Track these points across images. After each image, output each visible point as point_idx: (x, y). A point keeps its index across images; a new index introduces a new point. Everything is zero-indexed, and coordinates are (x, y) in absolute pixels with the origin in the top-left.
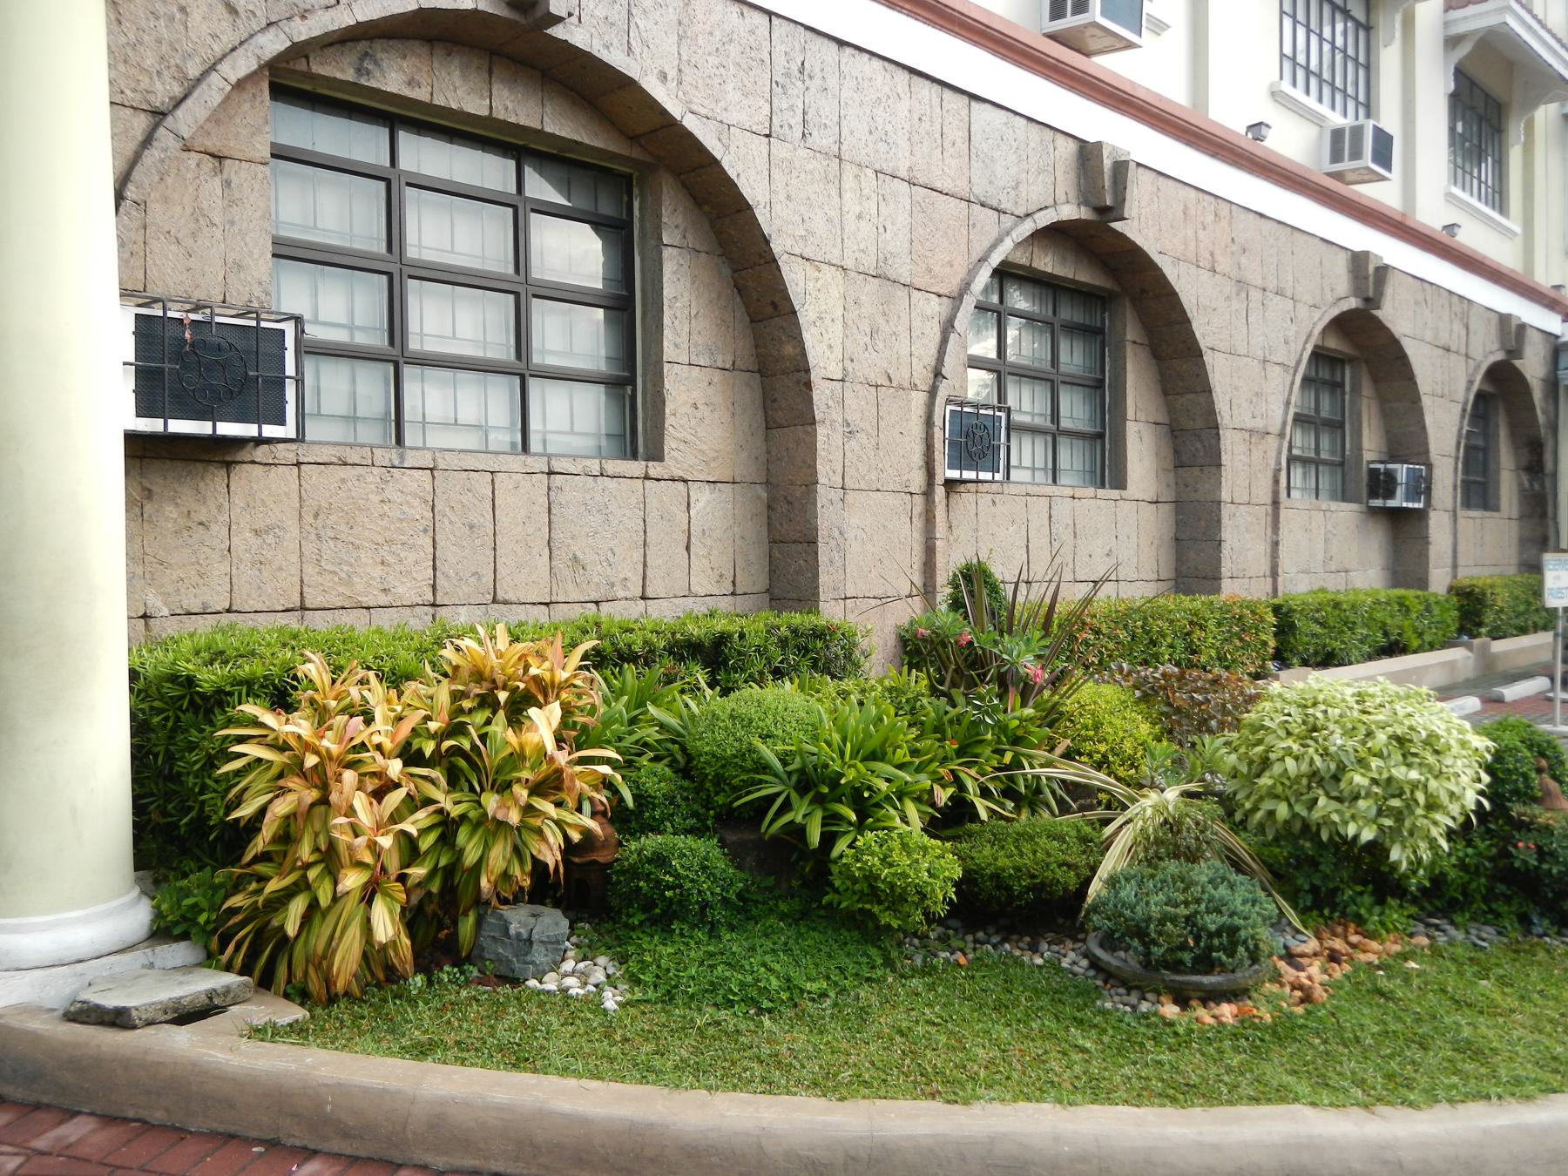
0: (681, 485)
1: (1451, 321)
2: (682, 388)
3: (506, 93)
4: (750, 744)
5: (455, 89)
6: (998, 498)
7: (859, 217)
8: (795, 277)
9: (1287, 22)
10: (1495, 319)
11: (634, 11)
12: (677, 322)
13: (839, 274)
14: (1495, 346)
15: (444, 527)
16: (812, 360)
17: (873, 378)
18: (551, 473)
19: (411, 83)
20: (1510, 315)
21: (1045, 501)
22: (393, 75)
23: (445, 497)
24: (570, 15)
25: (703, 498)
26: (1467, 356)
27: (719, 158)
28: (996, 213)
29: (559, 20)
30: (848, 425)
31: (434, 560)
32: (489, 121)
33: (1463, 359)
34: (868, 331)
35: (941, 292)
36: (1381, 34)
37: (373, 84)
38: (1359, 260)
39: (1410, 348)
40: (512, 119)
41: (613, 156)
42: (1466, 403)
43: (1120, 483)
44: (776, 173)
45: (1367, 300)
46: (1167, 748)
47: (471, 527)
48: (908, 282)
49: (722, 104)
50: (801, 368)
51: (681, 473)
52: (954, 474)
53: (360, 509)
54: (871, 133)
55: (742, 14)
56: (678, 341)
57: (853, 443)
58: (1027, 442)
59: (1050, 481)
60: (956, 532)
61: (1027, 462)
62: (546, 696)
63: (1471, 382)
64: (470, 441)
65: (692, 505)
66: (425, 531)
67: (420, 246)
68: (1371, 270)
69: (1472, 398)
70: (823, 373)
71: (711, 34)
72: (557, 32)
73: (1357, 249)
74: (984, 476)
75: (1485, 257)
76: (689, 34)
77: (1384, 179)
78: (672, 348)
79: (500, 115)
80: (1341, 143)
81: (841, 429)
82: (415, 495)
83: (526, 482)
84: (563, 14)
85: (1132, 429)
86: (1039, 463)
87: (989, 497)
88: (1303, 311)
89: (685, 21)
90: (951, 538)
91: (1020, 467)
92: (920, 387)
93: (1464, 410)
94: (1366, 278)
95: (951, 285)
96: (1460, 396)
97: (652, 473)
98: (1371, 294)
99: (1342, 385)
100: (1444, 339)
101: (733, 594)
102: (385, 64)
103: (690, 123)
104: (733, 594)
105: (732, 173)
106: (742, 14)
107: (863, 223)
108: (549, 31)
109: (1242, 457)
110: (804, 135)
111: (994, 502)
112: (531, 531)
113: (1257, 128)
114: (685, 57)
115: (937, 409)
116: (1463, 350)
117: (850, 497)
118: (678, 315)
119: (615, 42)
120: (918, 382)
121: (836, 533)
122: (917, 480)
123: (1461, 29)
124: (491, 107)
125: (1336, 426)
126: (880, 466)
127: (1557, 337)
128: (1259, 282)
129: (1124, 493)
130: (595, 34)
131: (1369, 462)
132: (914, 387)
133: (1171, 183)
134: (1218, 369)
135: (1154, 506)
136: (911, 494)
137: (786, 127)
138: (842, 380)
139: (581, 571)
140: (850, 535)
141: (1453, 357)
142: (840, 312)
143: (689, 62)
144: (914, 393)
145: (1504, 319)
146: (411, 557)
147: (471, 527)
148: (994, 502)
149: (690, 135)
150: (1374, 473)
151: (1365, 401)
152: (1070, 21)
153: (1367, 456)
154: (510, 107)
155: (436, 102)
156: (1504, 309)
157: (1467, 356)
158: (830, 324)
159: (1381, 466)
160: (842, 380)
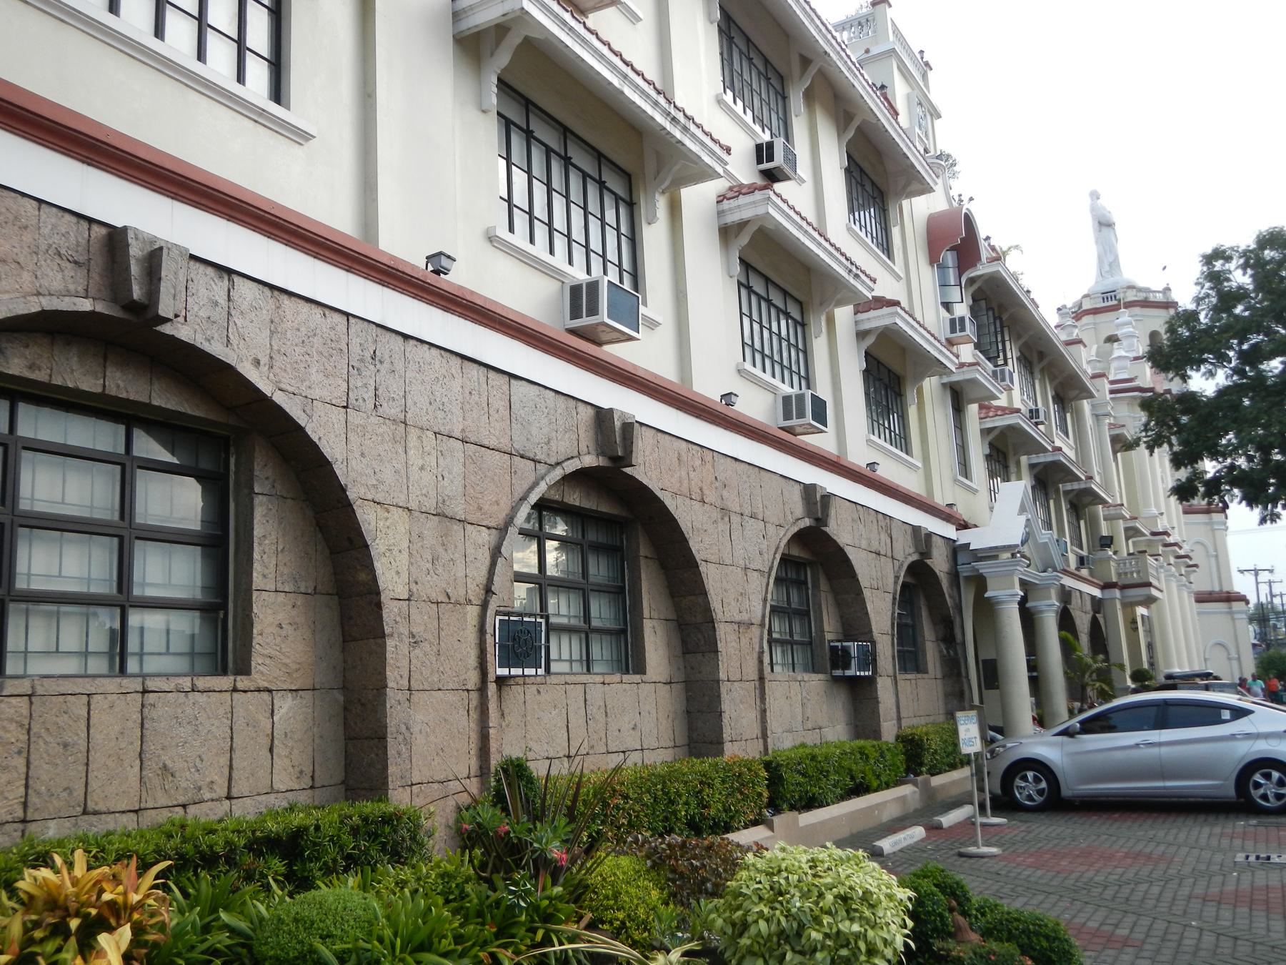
0: (266, 696)
1: (879, 533)
2: (269, 611)
3: (118, 374)
4: (311, 945)
5: (72, 371)
6: (542, 688)
7: (422, 468)
8: (367, 517)
9: (746, 321)
10: (909, 530)
11: (233, 312)
12: (265, 556)
13: (405, 514)
14: (912, 550)
15: (39, 748)
16: (382, 582)
17: (434, 597)
18: (145, 692)
19: (32, 367)
21: (581, 688)
22: (16, 361)
23: (41, 720)
24: (176, 316)
25: (285, 706)
26: (892, 558)
27: (303, 425)
28: (532, 463)
29: (167, 320)
30: (414, 636)
31: (27, 779)
32: (103, 396)
34: (430, 558)
36: (813, 328)
39: (852, 554)
40: (123, 395)
41: (212, 423)
42: (895, 594)
43: (640, 669)
44: (352, 436)
45: (817, 520)
46: (673, 910)
47: (66, 745)
48: (463, 517)
49: (307, 383)
50: (372, 592)
51: (266, 684)
52: (503, 672)
54: (431, 403)
55: (324, 315)
56: (266, 572)
57: (417, 651)
58: (565, 640)
60: (508, 718)
61: (565, 656)
62: (118, 918)
63: (897, 577)
64: (71, 666)
65: (276, 712)
66: (19, 752)
67: (32, 499)
68: (818, 498)
69: (899, 589)
70: (392, 595)
71: (299, 330)
72: (166, 329)
73: (807, 482)
74: (528, 671)
75: (898, 486)
76: (279, 330)
77: (822, 432)
78: (260, 578)
79: (112, 391)
80: (789, 406)
81: (407, 641)
82: (11, 720)
84: (171, 316)
85: (648, 625)
86: (576, 656)
87: (534, 688)
88: (771, 530)
89: (276, 320)
90: (504, 724)
91: (560, 660)
92: (474, 602)
93: (894, 599)
94: (816, 503)
95: (499, 518)
96: (891, 588)
97: (240, 685)
98: (820, 515)
99: (805, 583)
100: (875, 546)
101: (312, 787)
102: (8, 352)
103: (279, 398)
104: (312, 787)
105: (315, 438)
106: (324, 315)
107: (424, 473)
108: (158, 328)
109: (734, 644)
111: (539, 692)
112: (122, 746)
113: (728, 398)
114: (275, 347)
115: (489, 620)
116: (889, 554)
117: (416, 696)
118: (267, 550)
119: (216, 336)
120: (472, 598)
121: (403, 728)
122: (473, 678)
123: (867, 326)
124: (104, 386)
125: (804, 614)
126: (441, 669)
127: (954, 541)
128: (738, 509)
129: (645, 678)
130: (199, 330)
131: (829, 641)
132: (469, 602)
133: (667, 437)
134: (712, 577)
135: (668, 687)
136: (468, 690)
137: (361, 401)
138: (409, 600)
139: (170, 778)
140: (415, 729)
141: (883, 558)
142: (405, 544)
143: (279, 351)
144: (469, 607)
145: (916, 530)
147: (66, 745)
148: (539, 692)
149: (279, 408)
150: (834, 650)
151: (823, 594)
152: (585, 321)
153: (828, 636)
154: (122, 385)
155: (54, 382)
157: (892, 558)
158: (398, 554)
159: (839, 644)
160: (409, 600)
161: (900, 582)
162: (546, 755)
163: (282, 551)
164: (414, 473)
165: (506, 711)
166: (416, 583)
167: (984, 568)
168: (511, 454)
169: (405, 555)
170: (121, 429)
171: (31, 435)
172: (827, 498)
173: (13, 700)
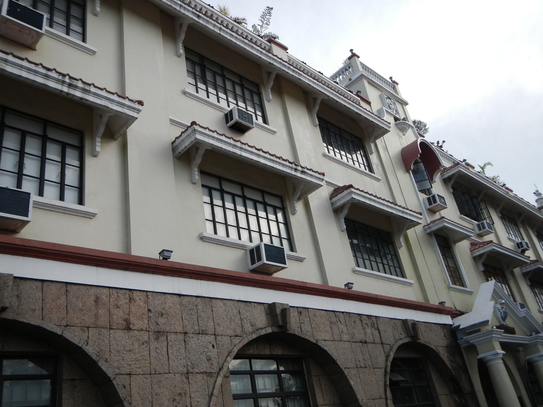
1: (364, 329)
10: (399, 324)
14: (403, 336)
20: (407, 319)
26: (382, 343)
33: (380, 347)
38: (271, 308)
45: (280, 327)
63: (387, 357)
69: (389, 364)
73: (270, 302)
75: (376, 295)
77: (283, 268)
93: (386, 371)
94: (277, 316)
96: (382, 363)
98: (280, 323)
100: (360, 336)
116: (378, 340)
123: (339, 204)
127: (451, 325)
133: (82, 286)
145: (405, 322)
151: (314, 378)
156: (404, 318)
157: (382, 343)
161: (391, 358)
167: (473, 339)
172: (285, 310)
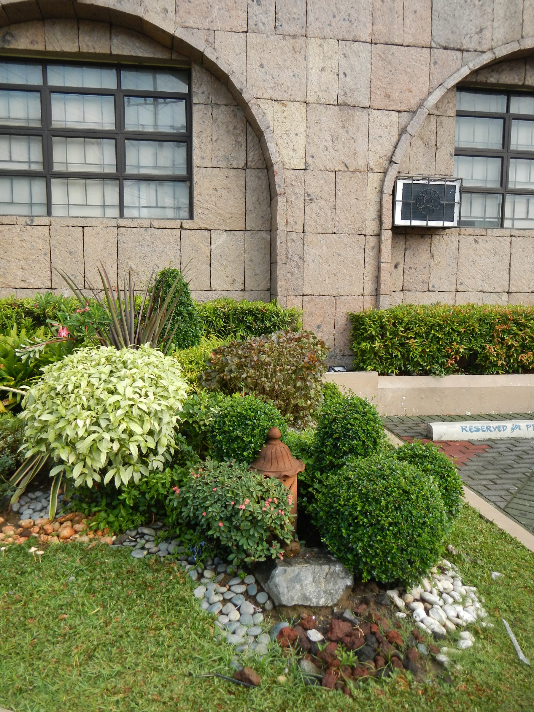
0: (206, 233)
2: (206, 180)
3: (87, 38)
6: (480, 239)
7: (323, 69)
12: (202, 145)
13: (303, 107)
15: (56, 253)
17: (330, 166)
18: (118, 227)
23: (56, 238)
27: (202, 50)
32: (80, 54)
34: (329, 138)
35: (399, 109)
37: (12, 46)
40: (92, 51)
41: (164, 61)
44: (251, 54)
47: (70, 253)
49: (209, 19)
51: (206, 226)
53: (9, 244)
54: (334, 16)
56: (204, 155)
57: (313, 206)
59: (46, 214)
64: (98, 212)
65: (213, 242)
66: (45, 254)
74: (447, 224)
78: (199, 159)
79: (84, 49)
81: (302, 199)
83: (104, 231)
90: (433, 263)
92: (376, 170)
95: (413, 103)
101: (244, 290)
104: (244, 290)
107: (324, 74)
110: (275, 27)
112: (106, 255)
117: (309, 237)
118: (204, 141)
120: (374, 167)
121: (296, 258)
122: (371, 227)
136: (365, 235)
137: (261, 24)
138: (305, 169)
139: (136, 275)
140: (308, 259)
142: (302, 128)
146: (38, 266)
147: (70, 253)
149: (181, 41)
155: (48, 49)
158: (295, 137)
162: (480, 289)
163: (216, 141)
164: (314, 73)
165: (436, 254)
166: (313, 157)
168: (431, 48)
169: (302, 137)
170: (505, 98)
171: (62, 85)
173: (40, 228)
